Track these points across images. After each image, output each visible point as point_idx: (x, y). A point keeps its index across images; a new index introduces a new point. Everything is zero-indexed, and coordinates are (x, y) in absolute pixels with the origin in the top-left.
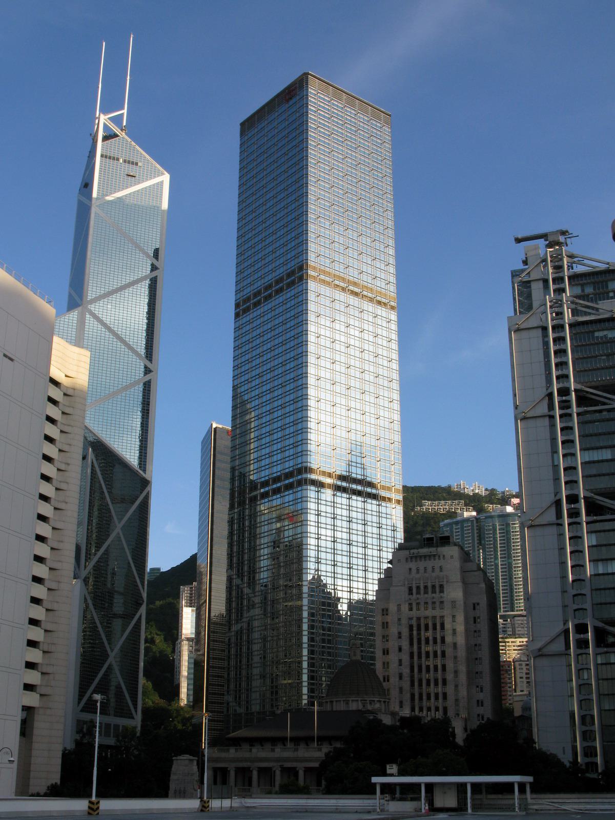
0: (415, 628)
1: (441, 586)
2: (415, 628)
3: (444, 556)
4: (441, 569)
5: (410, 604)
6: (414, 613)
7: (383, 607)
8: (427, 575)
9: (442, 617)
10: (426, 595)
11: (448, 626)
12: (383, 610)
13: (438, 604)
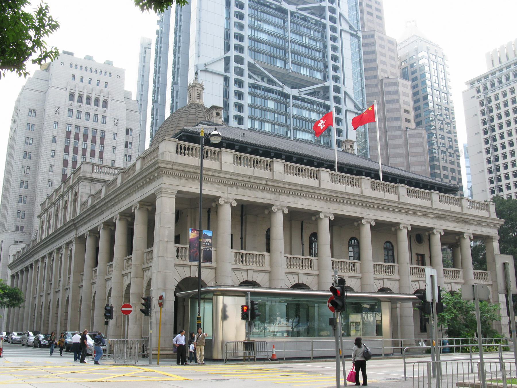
0: (72, 136)
1: (105, 103)
2: (72, 136)
3: (110, 74)
4: (106, 84)
5: (71, 110)
6: (74, 121)
7: (30, 107)
8: (90, 86)
9: (103, 132)
10: (88, 106)
11: (107, 141)
12: (30, 110)
13: (100, 117)
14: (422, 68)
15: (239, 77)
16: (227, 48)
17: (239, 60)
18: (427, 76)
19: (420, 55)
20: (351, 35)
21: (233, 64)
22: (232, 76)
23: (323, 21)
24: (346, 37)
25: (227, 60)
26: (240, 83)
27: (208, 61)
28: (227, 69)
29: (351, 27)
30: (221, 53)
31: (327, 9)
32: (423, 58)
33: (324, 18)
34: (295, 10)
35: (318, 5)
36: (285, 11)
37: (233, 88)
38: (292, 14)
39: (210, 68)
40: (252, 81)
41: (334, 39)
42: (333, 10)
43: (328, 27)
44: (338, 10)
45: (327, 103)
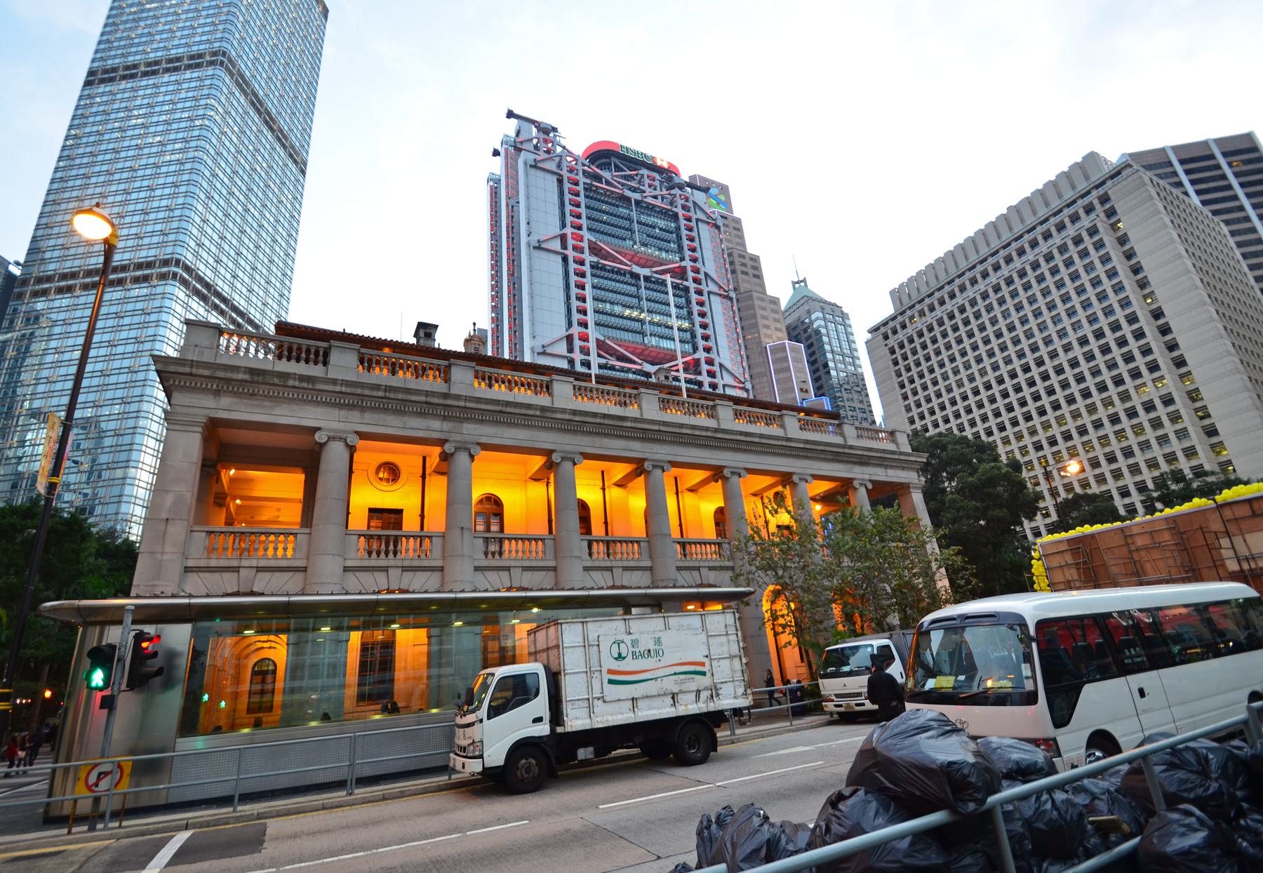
14: (817, 332)
18: (825, 339)
19: (813, 317)
21: (577, 343)
23: (685, 283)
24: (717, 303)
25: (569, 339)
27: (546, 342)
28: (570, 350)
30: (562, 332)
31: (689, 269)
32: (817, 319)
34: (649, 274)
38: (647, 279)
39: (549, 350)
40: (603, 361)
41: (701, 304)
42: (697, 271)
43: (692, 291)
45: (699, 378)
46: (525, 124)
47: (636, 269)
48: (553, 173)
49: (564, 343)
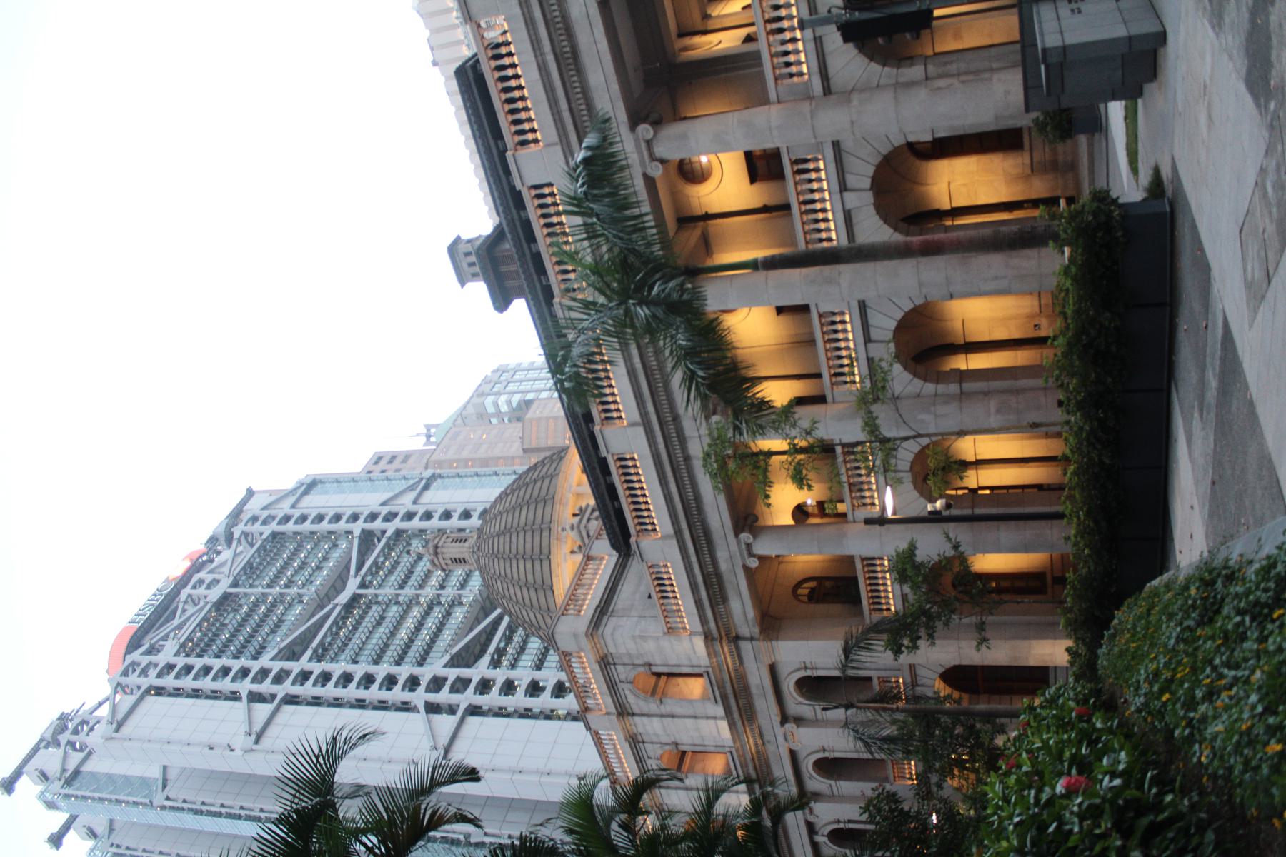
15: (473, 685)
16: (405, 707)
17: (436, 684)
19: (491, 409)
20: (426, 487)
21: (443, 697)
22: (469, 697)
24: (428, 497)
25: (433, 708)
26: (484, 686)
28: (452, 710)
29: (411, 488)
30: (417, 721)
32: (496, 404)
33: (384, 532)
34: (359, 579)
35: (356, 542)
36: (355, 599)
37: (493, 698)
38: (363, 585)
41: (428, 516)
44: (376, 509)
46: (35, 763)
47: (343, 598)
48: (141, 699)
49: (436, 718)
